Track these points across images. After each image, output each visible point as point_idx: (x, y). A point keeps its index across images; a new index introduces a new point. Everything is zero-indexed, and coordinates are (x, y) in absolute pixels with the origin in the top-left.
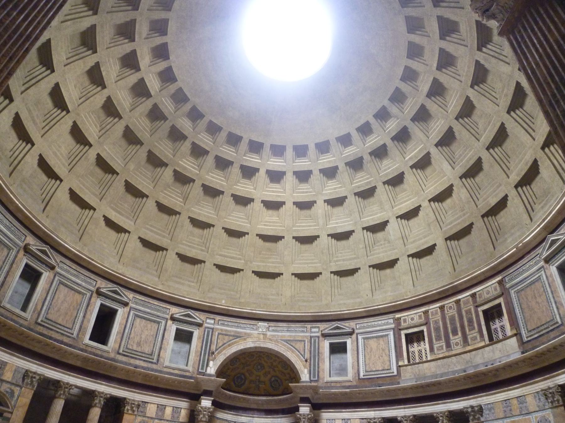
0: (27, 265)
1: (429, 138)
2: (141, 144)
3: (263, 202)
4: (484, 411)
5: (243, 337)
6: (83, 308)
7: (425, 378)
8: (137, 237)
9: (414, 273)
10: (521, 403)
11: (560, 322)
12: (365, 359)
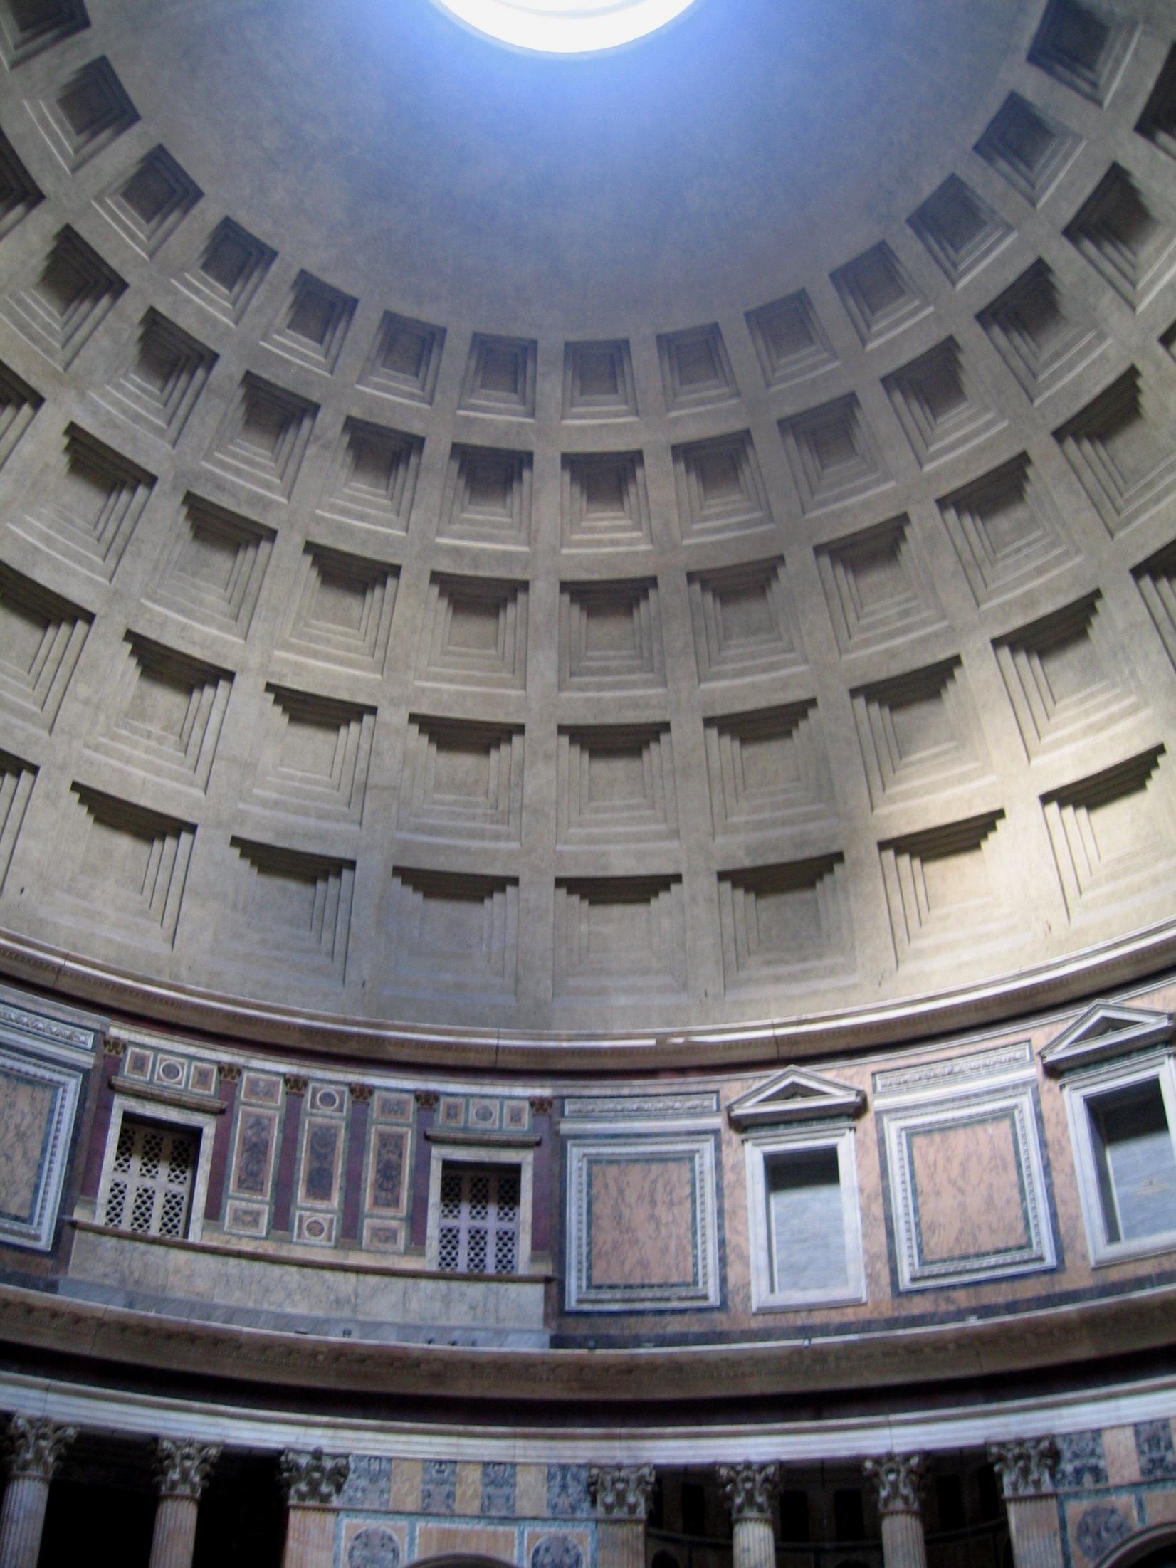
4: (351, 1476)
7: (161, 1301)
10: (492, 1482)
11: (714, 1299)
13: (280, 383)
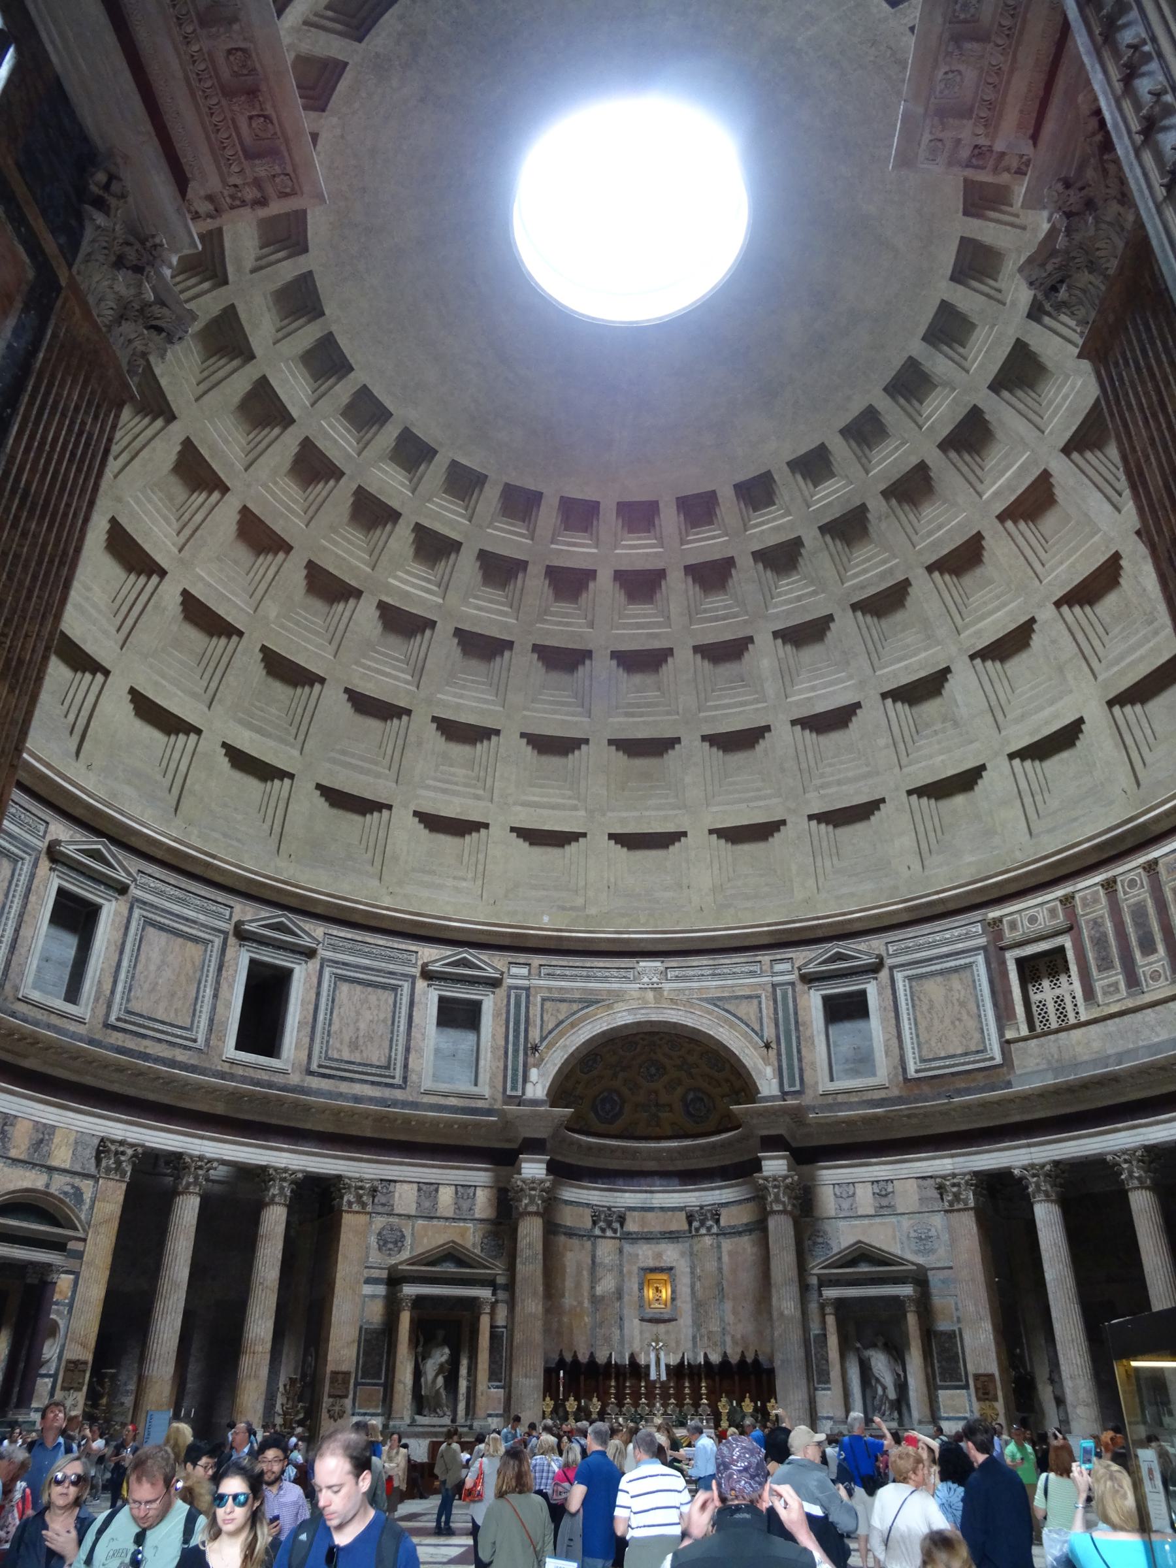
0: (61, 892)
1: (1043, 432)
2: (288, 548)
3: (615, 655)
5: (603, 1000)
6: (211, 975)
7: (1076, 1065)
8: (312, 785)
9: (1028, 800)
12: (917, 1029)
13: (838, 515)
